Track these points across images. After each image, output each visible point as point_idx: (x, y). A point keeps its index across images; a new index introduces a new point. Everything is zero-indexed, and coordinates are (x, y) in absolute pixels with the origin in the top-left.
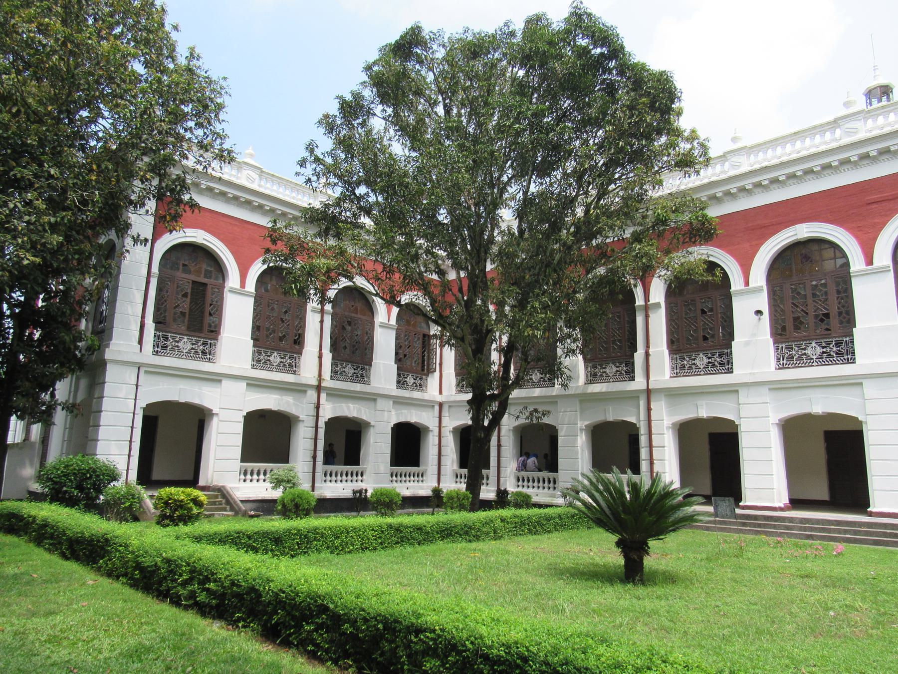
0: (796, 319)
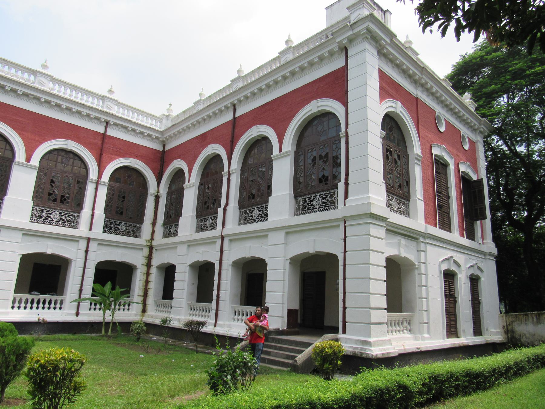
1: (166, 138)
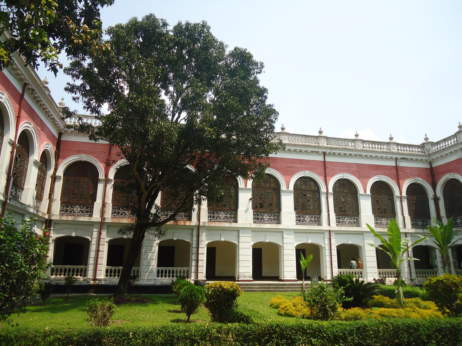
0: (261, 204)
1: (433, 159)
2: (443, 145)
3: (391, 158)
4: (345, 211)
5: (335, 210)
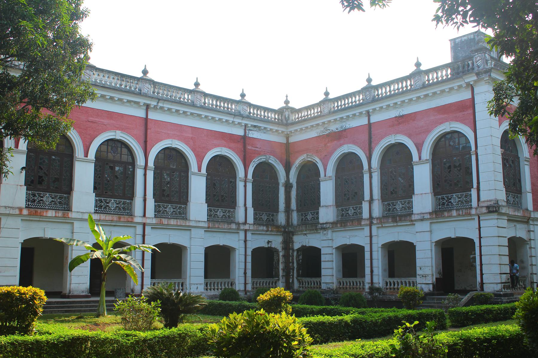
1: (291, 132)
2: (304, 113)
3: (239, 123)
4: (168, 196)
5: (154, 195)
